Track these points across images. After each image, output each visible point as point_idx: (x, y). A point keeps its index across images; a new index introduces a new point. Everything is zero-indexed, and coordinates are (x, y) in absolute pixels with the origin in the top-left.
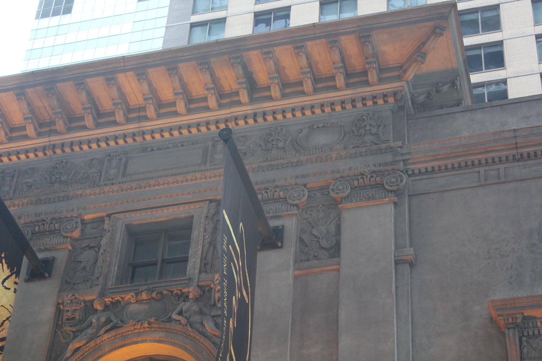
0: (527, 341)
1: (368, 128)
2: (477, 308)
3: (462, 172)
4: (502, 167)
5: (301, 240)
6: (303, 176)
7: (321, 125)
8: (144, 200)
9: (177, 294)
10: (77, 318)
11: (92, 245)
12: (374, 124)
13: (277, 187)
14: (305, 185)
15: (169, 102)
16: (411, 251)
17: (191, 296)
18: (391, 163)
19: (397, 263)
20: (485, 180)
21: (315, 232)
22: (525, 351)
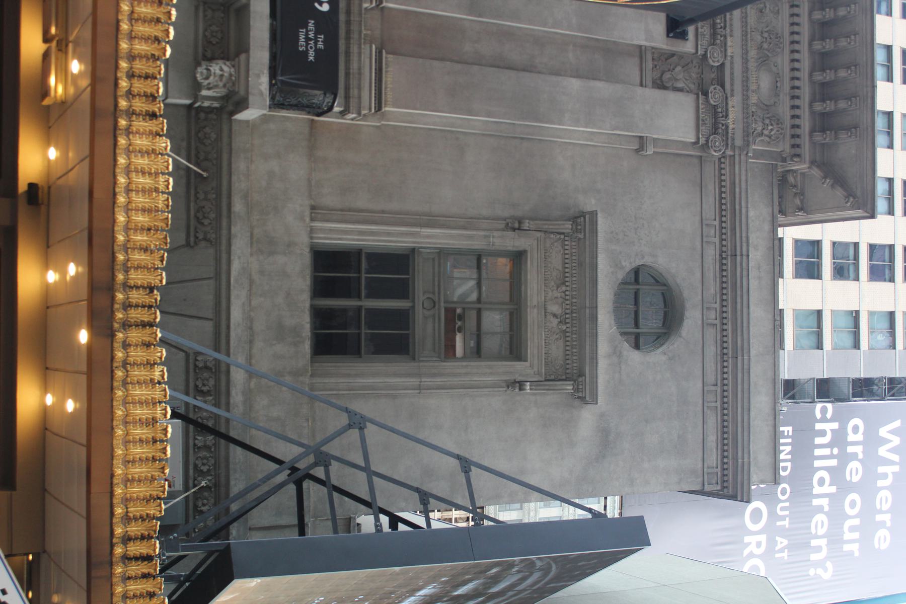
0: (560, 239)
1: (770, 128)
2: (593, 201)
3: (717, 206)
4: (717, 240)
5: (673, 55)
6: (732, 63)
7: (779, 84)
12: (772, 133)
13: (725, 37)
14: (723, 65)
16: (650, 152)
18: (733, 144)
19: (641, 137)
20: (707, 225)
21: (679, 68)
22: (552, 236)
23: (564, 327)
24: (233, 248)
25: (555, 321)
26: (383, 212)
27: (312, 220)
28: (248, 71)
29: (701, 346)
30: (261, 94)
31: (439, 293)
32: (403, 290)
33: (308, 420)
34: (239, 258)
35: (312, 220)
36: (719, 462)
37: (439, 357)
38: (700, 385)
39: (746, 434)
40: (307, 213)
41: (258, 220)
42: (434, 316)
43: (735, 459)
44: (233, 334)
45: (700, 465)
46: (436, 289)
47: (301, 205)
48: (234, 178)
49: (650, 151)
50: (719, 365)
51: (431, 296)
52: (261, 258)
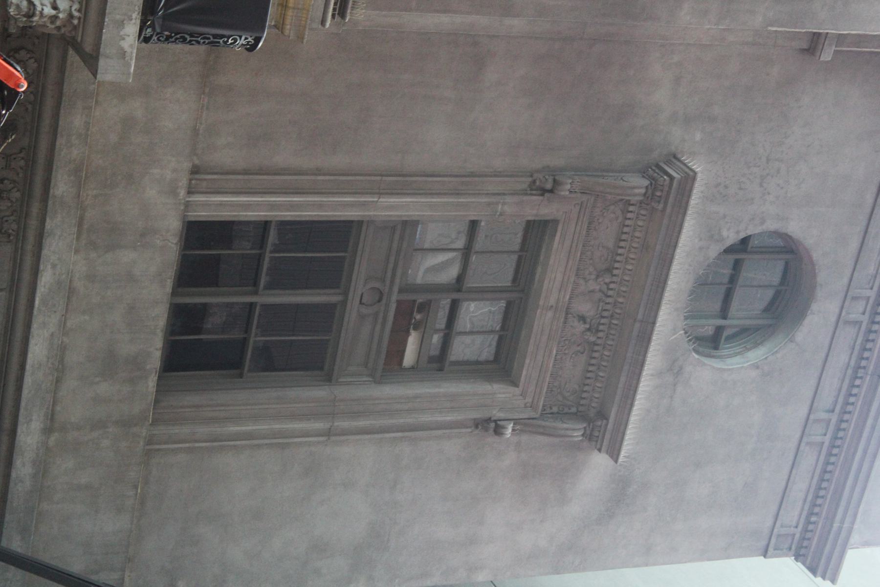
23: (592, 339)
24: (45, 252)
25: (581, 327)
26: (318, 172)
27: (190, 193)
28: (102, 13)
29: (823, 355)
30: (123, 54)
31: (392, 282)
32: (333, 275)
33: (136, 487)
34: (54, 266)
35: (190, 193)
36: (802, 520)
37: (372, 375)
38: (804, 410)
39: (858, 489)
40: (184, 182)
41: (96, 197)
42: (376, 315)
43: (831, 518)
44: (28, 380)
45: (769, 523)
46: (389, 274)
47: (175, 170)
48: (61, 141)
49: (827, 55)
50: (847, 381)
51: (377, 285)
52: (93, 255)
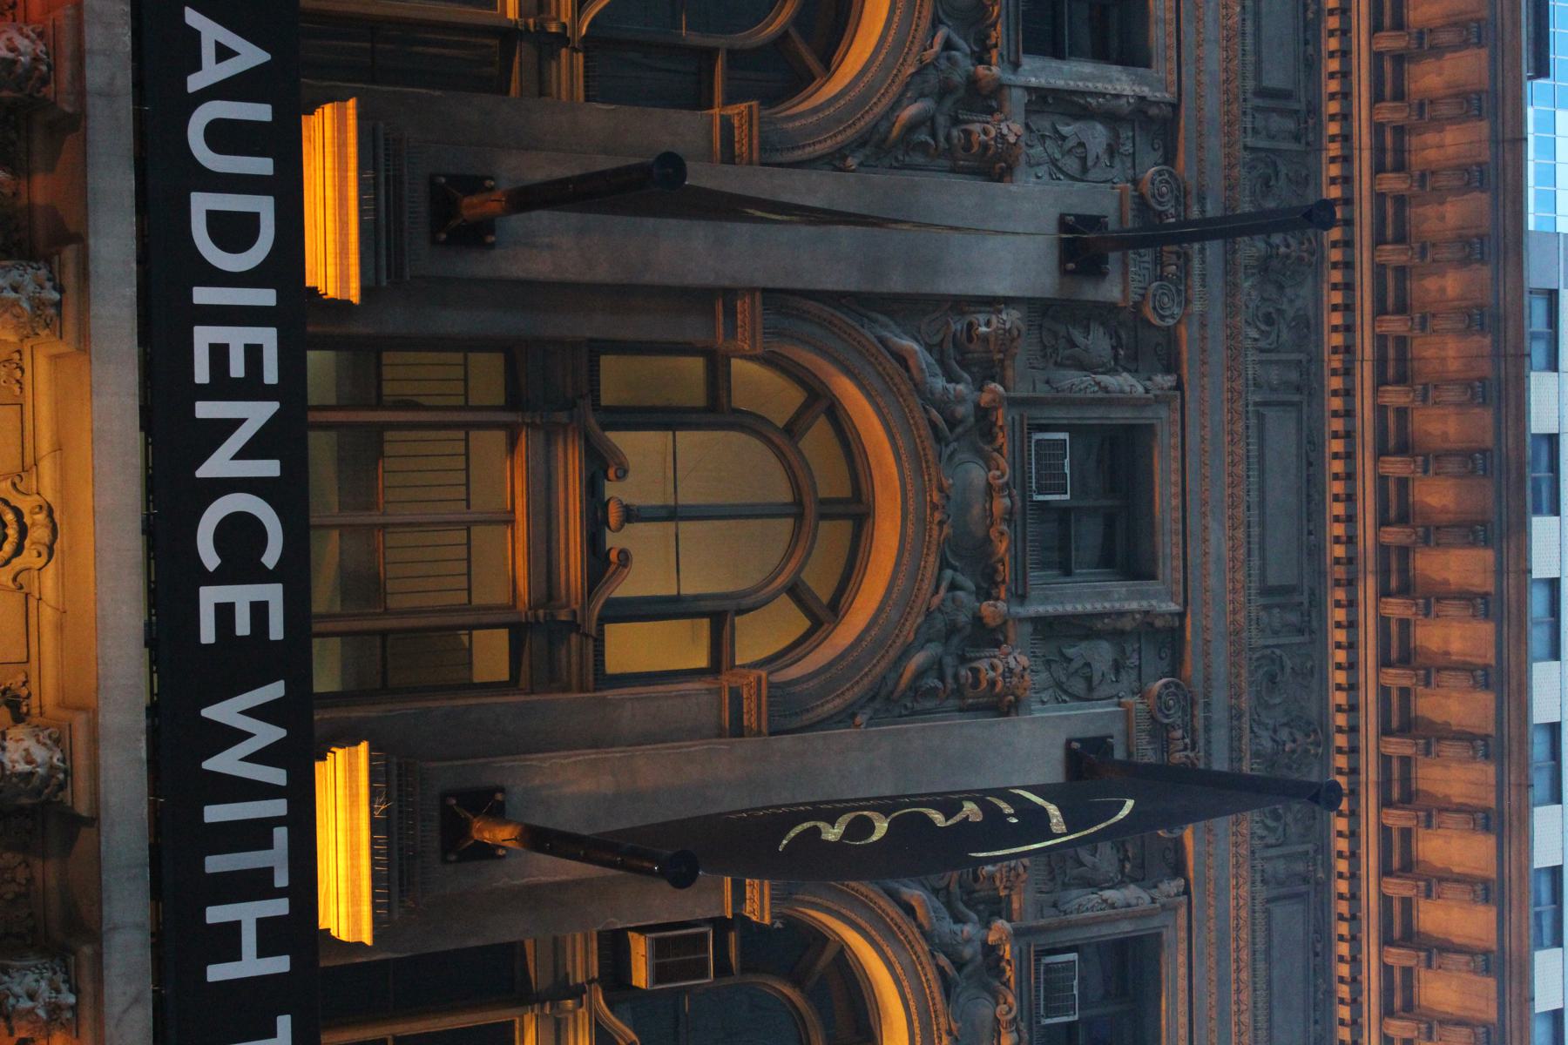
8: (1203, 338)
9: (988, 37)
10: (977, 887)
11: (1128, 866)
15: (1414, 841)
17: (981, 69)
